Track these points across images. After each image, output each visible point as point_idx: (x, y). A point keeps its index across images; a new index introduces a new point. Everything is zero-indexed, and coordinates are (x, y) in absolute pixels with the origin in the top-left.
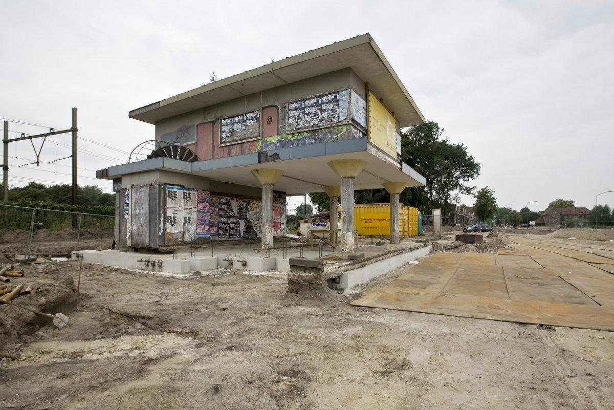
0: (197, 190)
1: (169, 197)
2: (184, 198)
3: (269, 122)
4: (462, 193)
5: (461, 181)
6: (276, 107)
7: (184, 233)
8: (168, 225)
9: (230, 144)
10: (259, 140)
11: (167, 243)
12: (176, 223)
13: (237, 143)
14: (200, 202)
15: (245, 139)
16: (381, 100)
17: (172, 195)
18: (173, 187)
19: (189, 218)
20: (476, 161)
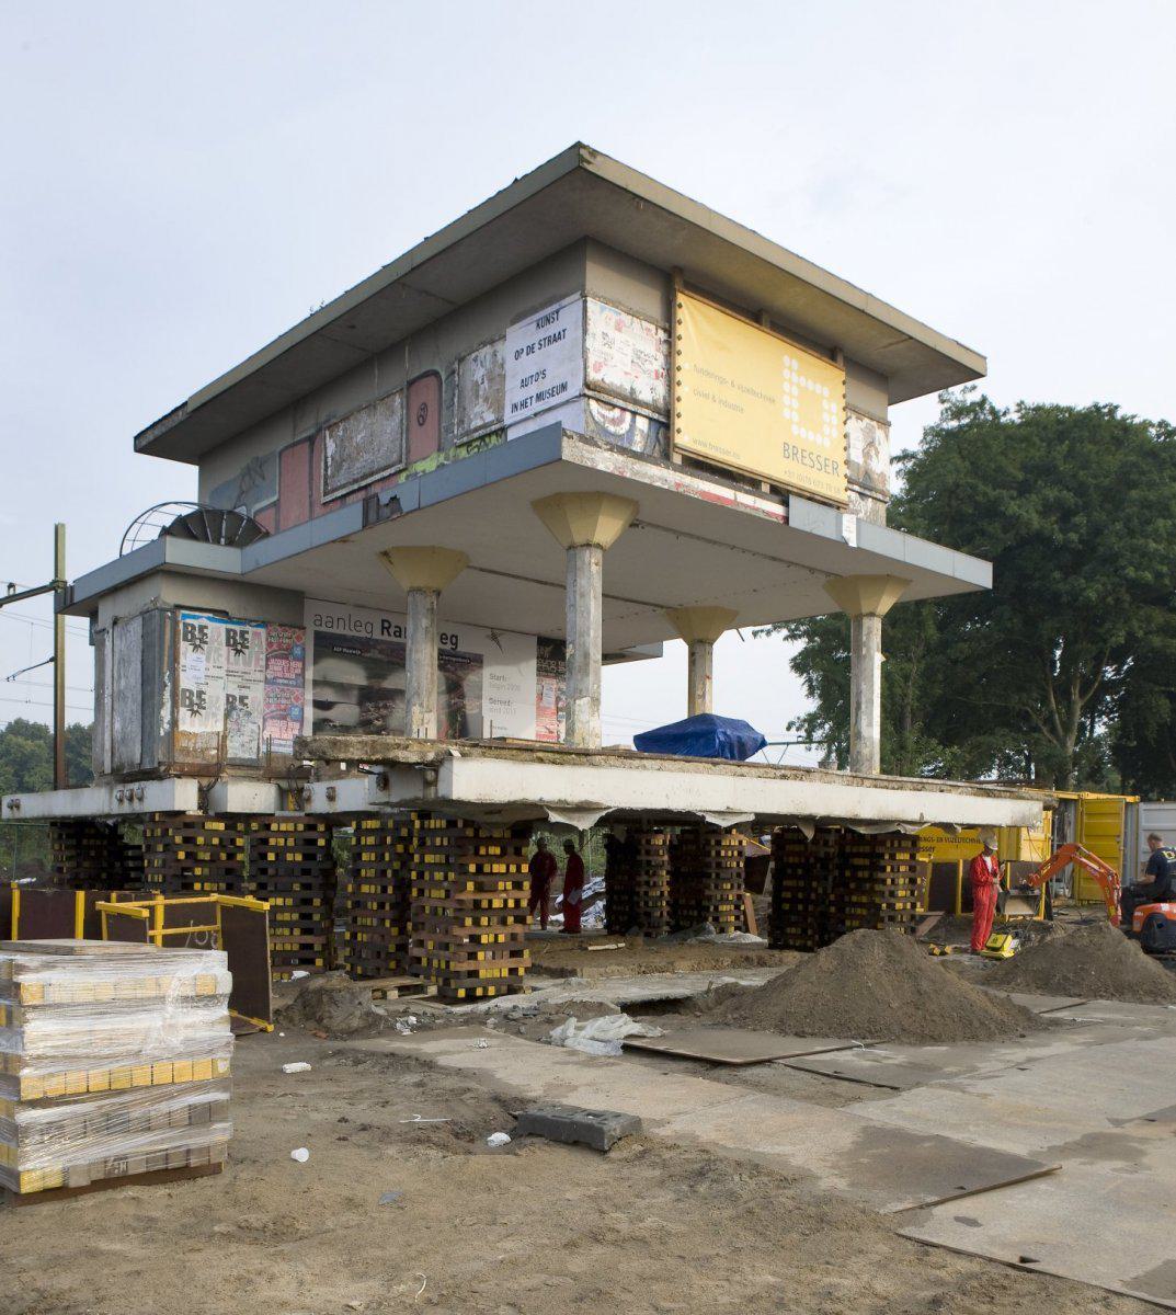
0: (264, 624)
1: (185, 639)
2: (228, 644)
3: (422, 420)
6: (436, 374)
7: (225, 737)
8: (184, 713)
9: (344, 492)
10: (400, 471)
12: (204, 708)
13: (356, 487)
14: (276, 657)
15: (372, 474)
17: (193, 636)
18: (197, 614)
19: (242, 699)
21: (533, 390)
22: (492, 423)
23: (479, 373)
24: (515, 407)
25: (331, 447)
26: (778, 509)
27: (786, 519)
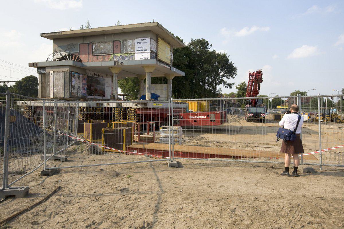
0: (82, 75)
2: (78, 77)
3: (117, 47)
4: (226, 87)
5: (225, 79)
6: (120, 41)
11: (72, 97)
13: (101, 55)
15: (105, 53)
16: (163, 39)
19: (79, 87)
20: (235, 66)
21: (141, 49)
22: (132, 52)
23: (130, 44)
24: (137, 51)
25: (94, 47)
26: (169, 68)
27: (170, 69)
